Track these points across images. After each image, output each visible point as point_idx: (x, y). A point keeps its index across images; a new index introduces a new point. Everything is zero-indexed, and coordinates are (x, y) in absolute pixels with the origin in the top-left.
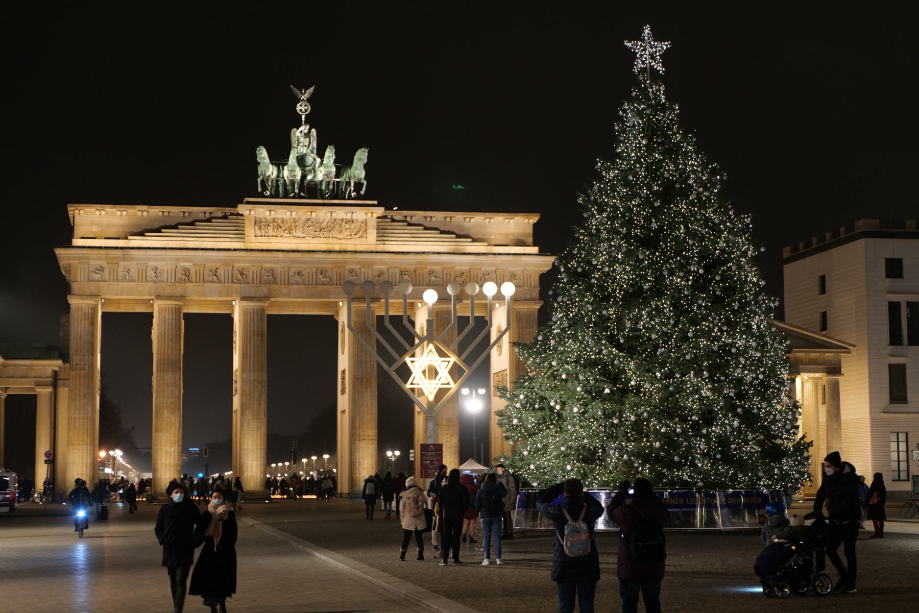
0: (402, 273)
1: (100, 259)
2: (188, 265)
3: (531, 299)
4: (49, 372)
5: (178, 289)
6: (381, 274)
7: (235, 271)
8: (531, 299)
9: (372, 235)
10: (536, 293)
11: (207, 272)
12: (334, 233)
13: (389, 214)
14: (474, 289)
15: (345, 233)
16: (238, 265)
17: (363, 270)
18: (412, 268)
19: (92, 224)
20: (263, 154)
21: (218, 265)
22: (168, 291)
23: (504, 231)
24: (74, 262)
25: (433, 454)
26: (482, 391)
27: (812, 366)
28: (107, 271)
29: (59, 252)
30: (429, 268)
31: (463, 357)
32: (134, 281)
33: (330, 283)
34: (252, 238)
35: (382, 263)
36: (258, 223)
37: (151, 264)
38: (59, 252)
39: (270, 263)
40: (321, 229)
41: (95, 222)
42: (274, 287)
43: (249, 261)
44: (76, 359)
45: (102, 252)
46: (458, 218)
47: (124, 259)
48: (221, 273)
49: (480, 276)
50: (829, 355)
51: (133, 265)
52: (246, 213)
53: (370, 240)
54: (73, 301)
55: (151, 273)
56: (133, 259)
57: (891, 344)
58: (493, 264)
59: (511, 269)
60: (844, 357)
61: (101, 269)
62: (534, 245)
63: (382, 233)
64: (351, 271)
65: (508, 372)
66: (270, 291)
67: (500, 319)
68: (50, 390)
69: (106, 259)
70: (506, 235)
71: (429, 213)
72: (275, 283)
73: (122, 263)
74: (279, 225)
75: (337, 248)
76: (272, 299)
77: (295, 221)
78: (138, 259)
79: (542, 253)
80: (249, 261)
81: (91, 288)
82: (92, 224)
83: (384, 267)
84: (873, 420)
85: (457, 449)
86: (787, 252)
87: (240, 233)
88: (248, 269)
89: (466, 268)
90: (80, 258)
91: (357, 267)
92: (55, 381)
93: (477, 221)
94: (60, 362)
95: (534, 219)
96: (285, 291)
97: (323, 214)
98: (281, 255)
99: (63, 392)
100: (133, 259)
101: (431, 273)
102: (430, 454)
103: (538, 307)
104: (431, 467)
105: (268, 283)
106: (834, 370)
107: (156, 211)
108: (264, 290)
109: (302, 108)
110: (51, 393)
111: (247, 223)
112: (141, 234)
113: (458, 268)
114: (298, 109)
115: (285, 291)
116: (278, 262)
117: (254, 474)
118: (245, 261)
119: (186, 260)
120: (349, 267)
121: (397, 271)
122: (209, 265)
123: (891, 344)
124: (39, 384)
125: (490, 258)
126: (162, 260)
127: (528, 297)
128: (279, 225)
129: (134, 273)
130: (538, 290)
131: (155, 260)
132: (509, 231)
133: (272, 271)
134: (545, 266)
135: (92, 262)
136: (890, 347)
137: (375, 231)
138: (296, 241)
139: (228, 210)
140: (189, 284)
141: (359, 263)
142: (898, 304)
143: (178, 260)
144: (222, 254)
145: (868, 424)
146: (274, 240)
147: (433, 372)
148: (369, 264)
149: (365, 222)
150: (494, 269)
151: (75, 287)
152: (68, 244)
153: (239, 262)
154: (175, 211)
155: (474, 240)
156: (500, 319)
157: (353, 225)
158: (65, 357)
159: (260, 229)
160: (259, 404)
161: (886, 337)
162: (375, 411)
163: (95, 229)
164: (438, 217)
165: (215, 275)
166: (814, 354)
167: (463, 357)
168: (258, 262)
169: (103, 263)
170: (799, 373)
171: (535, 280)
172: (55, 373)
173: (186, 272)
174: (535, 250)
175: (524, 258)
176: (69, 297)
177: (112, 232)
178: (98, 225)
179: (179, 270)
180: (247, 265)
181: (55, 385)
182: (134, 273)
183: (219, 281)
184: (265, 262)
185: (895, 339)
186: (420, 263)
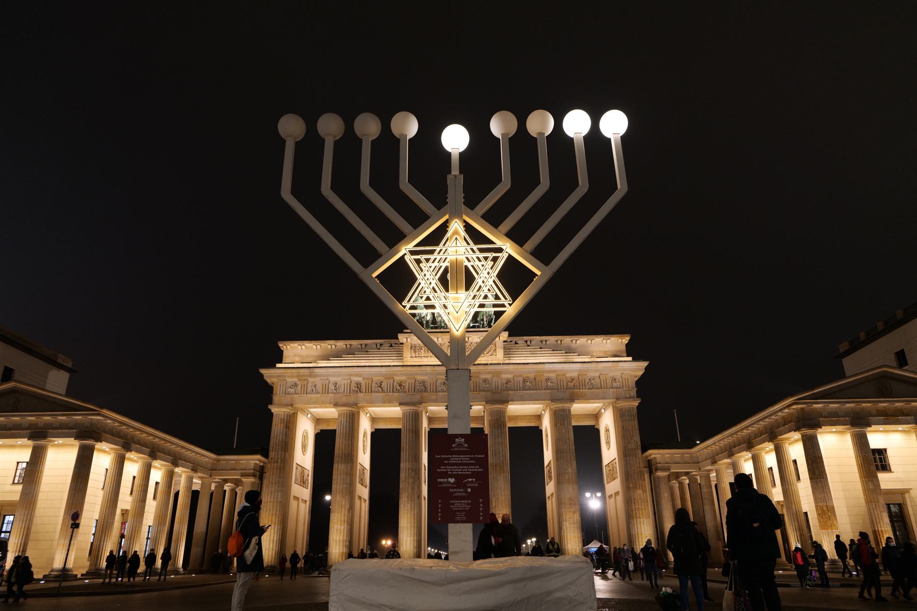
0: (524, 381)
1: (292, 377)
2: (360, 379)
3: (630, 397)
4: (252, 466)
5: (352, 399)
6: (508, 381)
8: (630, 397)
10: (634, 392)
11: (374, 385)
13: (514, 339)
14: (545, 123)
16: (397, 378)
17: (494, 379)
18: (532, 376)
19: (295, 355)
21: (382, 378)
22: (344, 400)
23: (603, 349)
24: (275, 380)
25: (465, 458)
26: (599, 494)
28: (299, 387)
29: (263, 371)
30: (546, 375)
31: (532, 243)
32: (318, 393)
34: (409, 358)
37: (332, 379)
38: (263, 371)
39: (421, 375)
41: (298, 353)
42: (425, 394)
43: (405, 375)
44: (272, 454)
45: (294, 371)
46: (567, 340)
47: (311, 376)
48: (384, 385)
49: (587, 381)
51: (318, 381)
54: (274, 409)
55: (332, 387)
56: (317, 376)
58: (597, 371)
59: (612, 374)
61: (296, 385)
62: (628, 356)
63: (508, 351)
64: (485, 381)
65: (617, 460)
66: (422, 398)
67: (607, 422)
68: (252, 479)
69: (298, 376)
70: (605, 352)
71: (544, 338)
72: (426, 390)
73: (311, 380)
78: (321, 376)
79: (634, 360)
80: (405, 375)
81: (288, 399)
82: (295, 355)
83: (510, 376)
85: (579, 525)
86: (844, 347)
87: (400, 355)
88: (405, 381)
89: (575, 375)
90: (278, 376)
91: (488, 376)
92: (260, 473)
94: (259, 457)
95: (626, 339)
96: (434, 397)
98: (428, 368)
99: (265, 482)
100: (317, 376)
101: (548, 380)
102: (455, 459)
103: (636, 403)
104: (459, 492)
105: (421, 391)
107: (341, 344)
108: (417, 397)
110: (253, 483)
111: (405, 348)
113: (568, 375)
115: (434, 397)
116: (426, 374)
117: (408, 549)
118: (402, 375)
119: (357, 375)
120: (483, 376)
121: (521, 379)
122: (375, 379)
124: (243, 475)
125: (594, 365)
126: (339, 376)
127: (628, 396)
129: (319, 387)
130: (635, 390)
131: (334, 376)
132: (607, 349)
133: (423, 383)
134: (639, 370)
135: (289, 380)
137: (502, 351)
139: (393, 341)
140: (360, 395)
141: (489, 373)
143: (351, 375)
144: (384, 369)
147: (458, 278)
148: (498, 374)
150: (597, 374)
151: (276, 398)
152: (274, 366)
153: (397, 375)
154: (355, 343)
156: (607, 422)
158: (266, 456)
159: (415, 352)
160: (413, 488)
162: (508, 493)
163: (297, 359)
164: (552, 339)
165: (380, 386)
167: (532, 243)
168: (411, 374)
169: (296, 380)
171: (632, 382)
172: (263, 467)
173: (358, 385)
174: (630, 359)
175: (621, 364)
176: (269, 407)
178: (299, 356)
179: (353, 384)
180: (403, 378)
181: (261, 478)
182: (319, 387)
183: (383, 391)
184: (417, 374)
186: (538, 372)
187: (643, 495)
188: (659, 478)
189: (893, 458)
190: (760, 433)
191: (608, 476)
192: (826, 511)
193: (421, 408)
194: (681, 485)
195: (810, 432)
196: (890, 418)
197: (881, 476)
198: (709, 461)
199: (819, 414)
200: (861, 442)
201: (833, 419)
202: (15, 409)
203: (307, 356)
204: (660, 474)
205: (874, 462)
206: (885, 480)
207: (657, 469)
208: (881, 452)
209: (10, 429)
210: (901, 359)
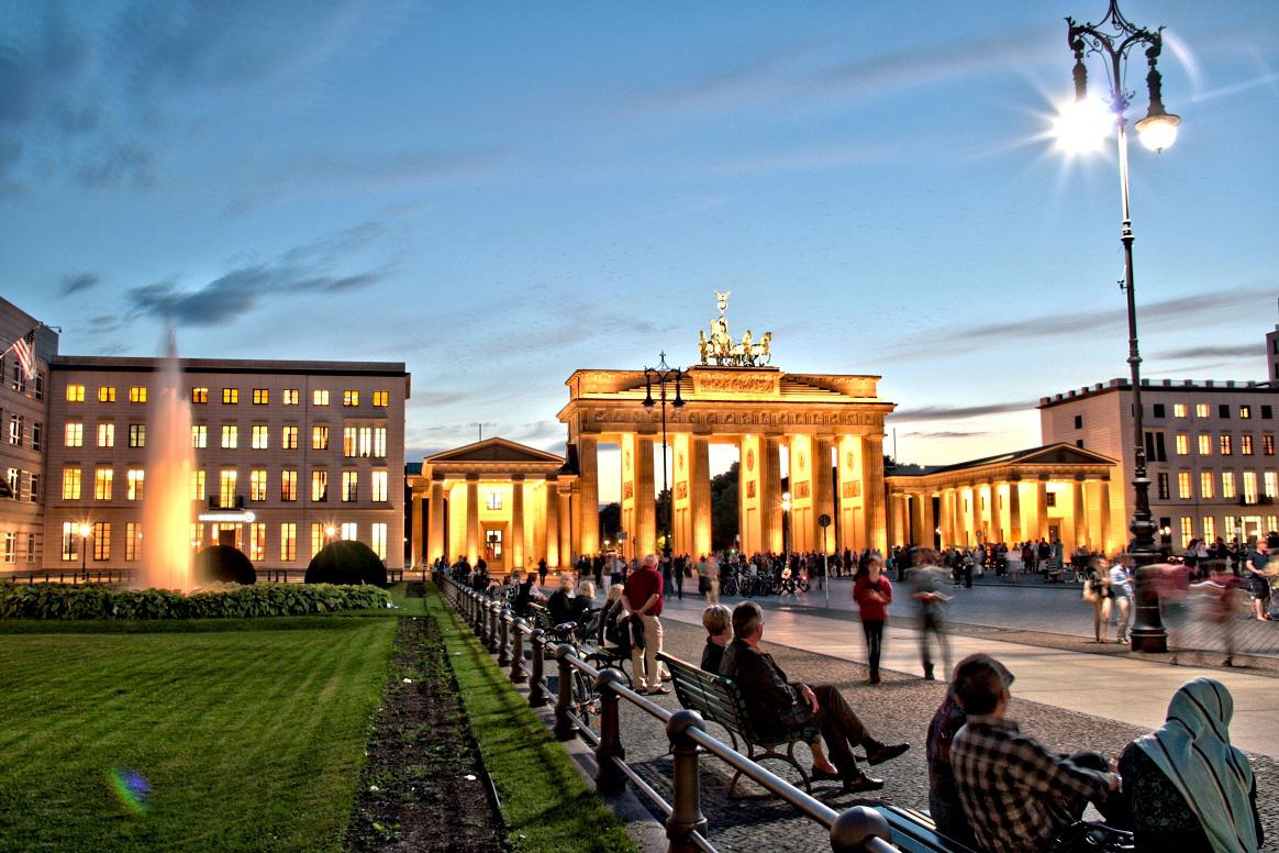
9: (777, 390)
12: (752, 389)
15: (760, 389)
27: (1093, 474)
35: (784, 410)
36: (703, 382)
40: (745, 386)
42: (714, 425)
44: (587, 475)
50: (1103, 467)
60: (1112, 469)
74: (717, 384)
75: (755, 399)
76: (714, 434)
82: (592, 383)
84: (1127, 510)
89: (837, 413)
91: (767, 412)
97: (745, 377)
98: (720, 404)
106: (1106, 477)
108: (709, 427)
111: (695, 383)
112: (627, 390)
115: (722, 428)
116: (718, 408)
118: (697, 408)
145: (1124, 513)
146: (713, 394)
149: (772, 382)
163: (594, 387)
166: (1094, 467)
170: (1084, 479)
177: (606, 389)
178: (597, 384)
187: (881, 511)
188: (894, 498)
189: (1058, 499)
190: (983, 477)
191: (845, 493)
192: (1015, 530)
194: (903, 500)
195: (1014, 483)
196: (1061, 475)
197: (1050, 509)
198: (936, 487)
199: (1022, 472)
200: (1042, 489)
201: (1030, 475)
202: (496, 458)
203: (604, 384)
204: (896, 495)
205: (1048, 500)
206: (1052, 512)
207: (893, 491)
208: (1052, 495)
209: (498, 472)
210: (1079, 423)
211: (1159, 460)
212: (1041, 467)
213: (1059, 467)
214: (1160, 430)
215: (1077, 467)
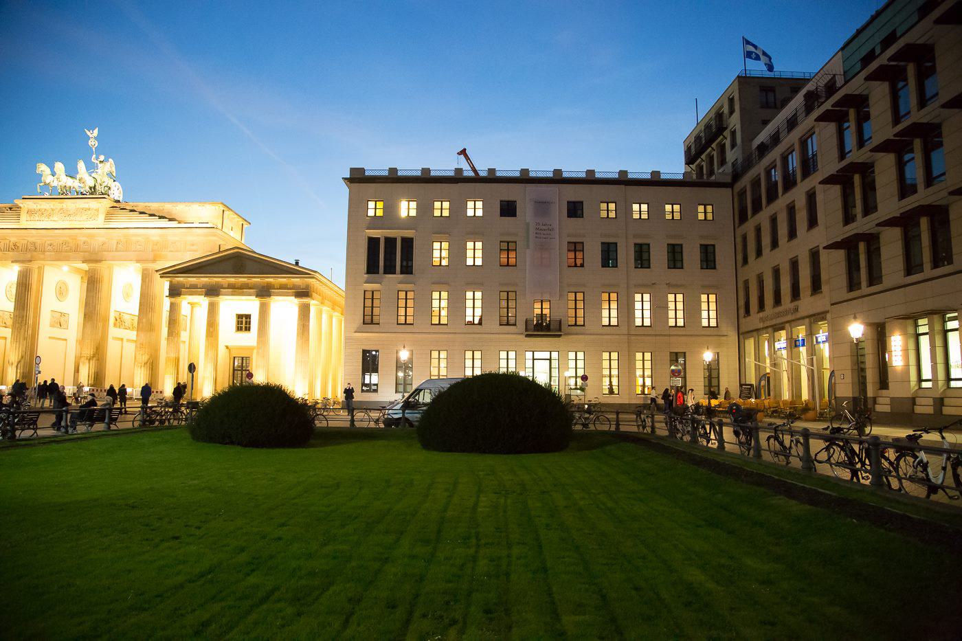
7: (11, 244)
9: (102, 217)
16: (13, 240)
20: (43, 168)
33: (71, 250)
40: (66, 213)
50: (296, 281)
52: (21, 205)
53: (100, 221)
57: (368, 272)
66: (32, 257)
77: (53, 210)
93: (179, 209)
96: (42, 256)
98: (33, 231)
108: (29, 256)
109: (93, 143)
111: (22, 212)
114: (90, 143)
123: (368, 272)
128: (41, 212)
136: (366, 276)
138: (54, 223)
142: (395, 239)
148: (92, 236)
149: (97, 210)
155: (170, 220)
157: (89, 212)
161: (363, 266)
166: (282, 280)
185: (372, 268)
193: (34, 266)
211: (402, 273)
212: (204, 280)
213: (232, 279)
214: (408, 233)
215: (257, 280)
